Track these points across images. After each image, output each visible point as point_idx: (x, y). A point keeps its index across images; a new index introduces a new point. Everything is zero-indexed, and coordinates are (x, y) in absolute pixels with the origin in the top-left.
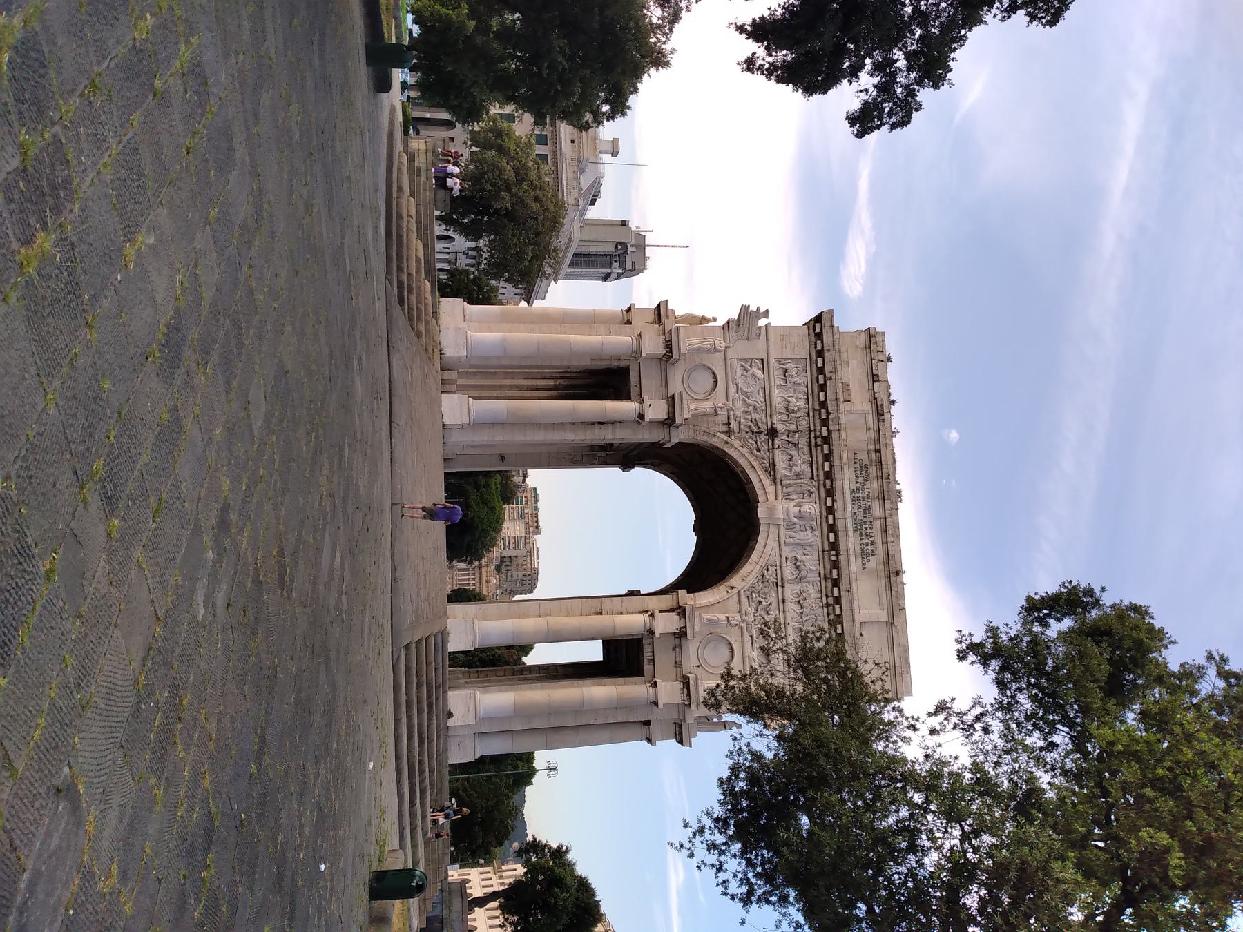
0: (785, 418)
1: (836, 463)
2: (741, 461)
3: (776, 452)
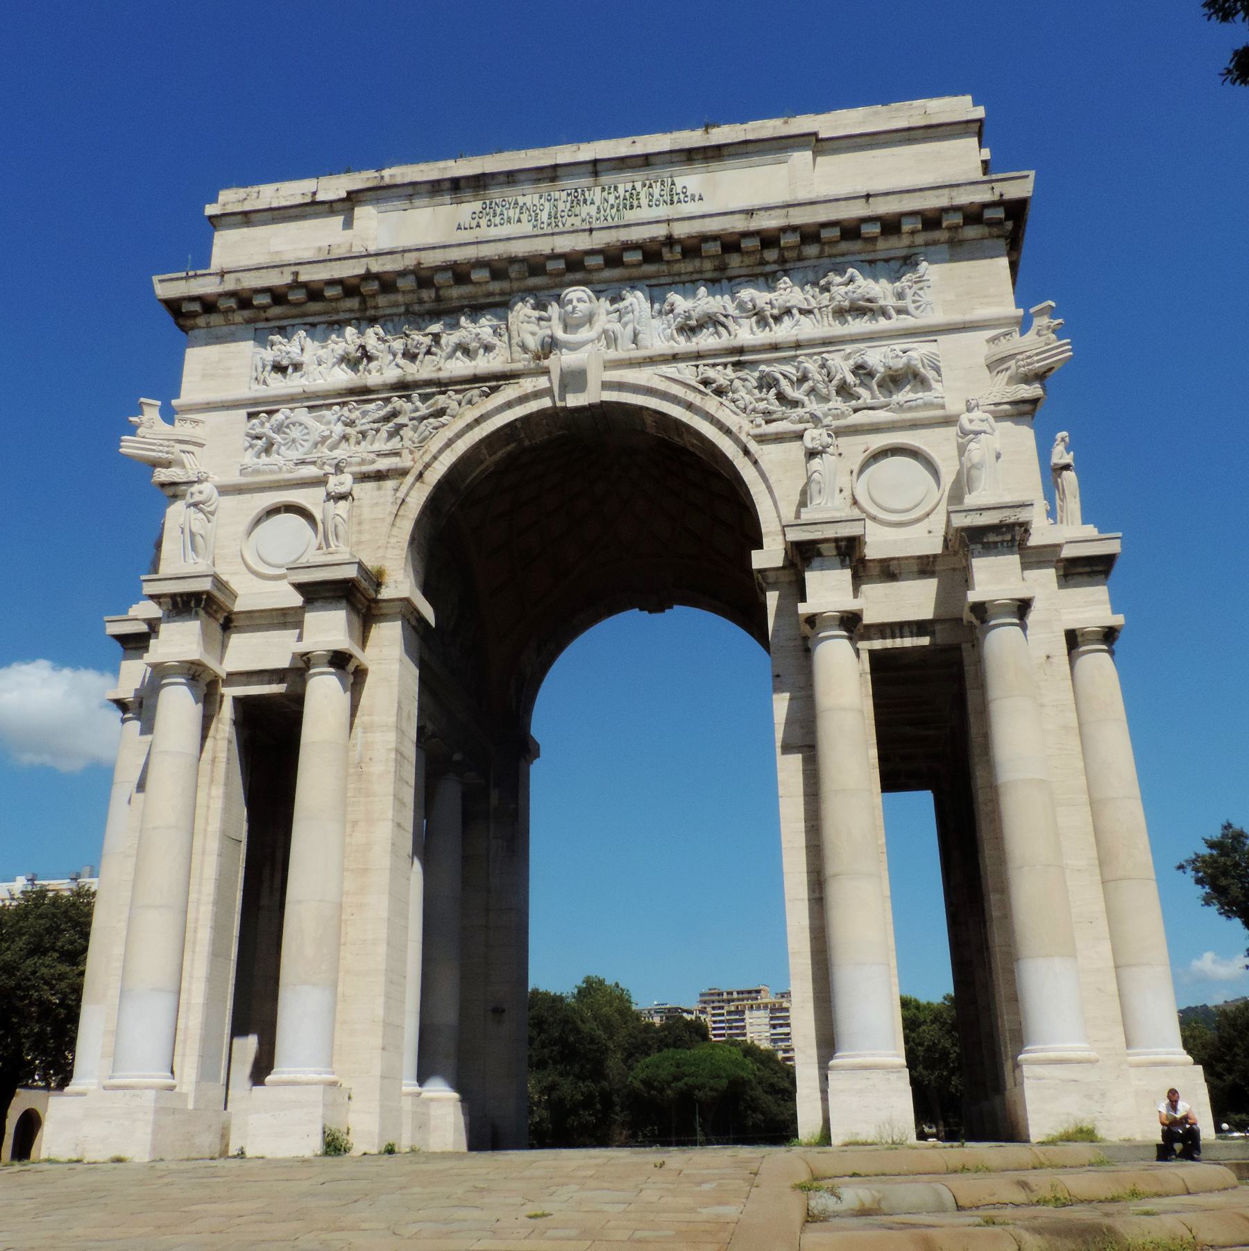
0: (373, 365)
1: (470, 253)
2: (462, 447)
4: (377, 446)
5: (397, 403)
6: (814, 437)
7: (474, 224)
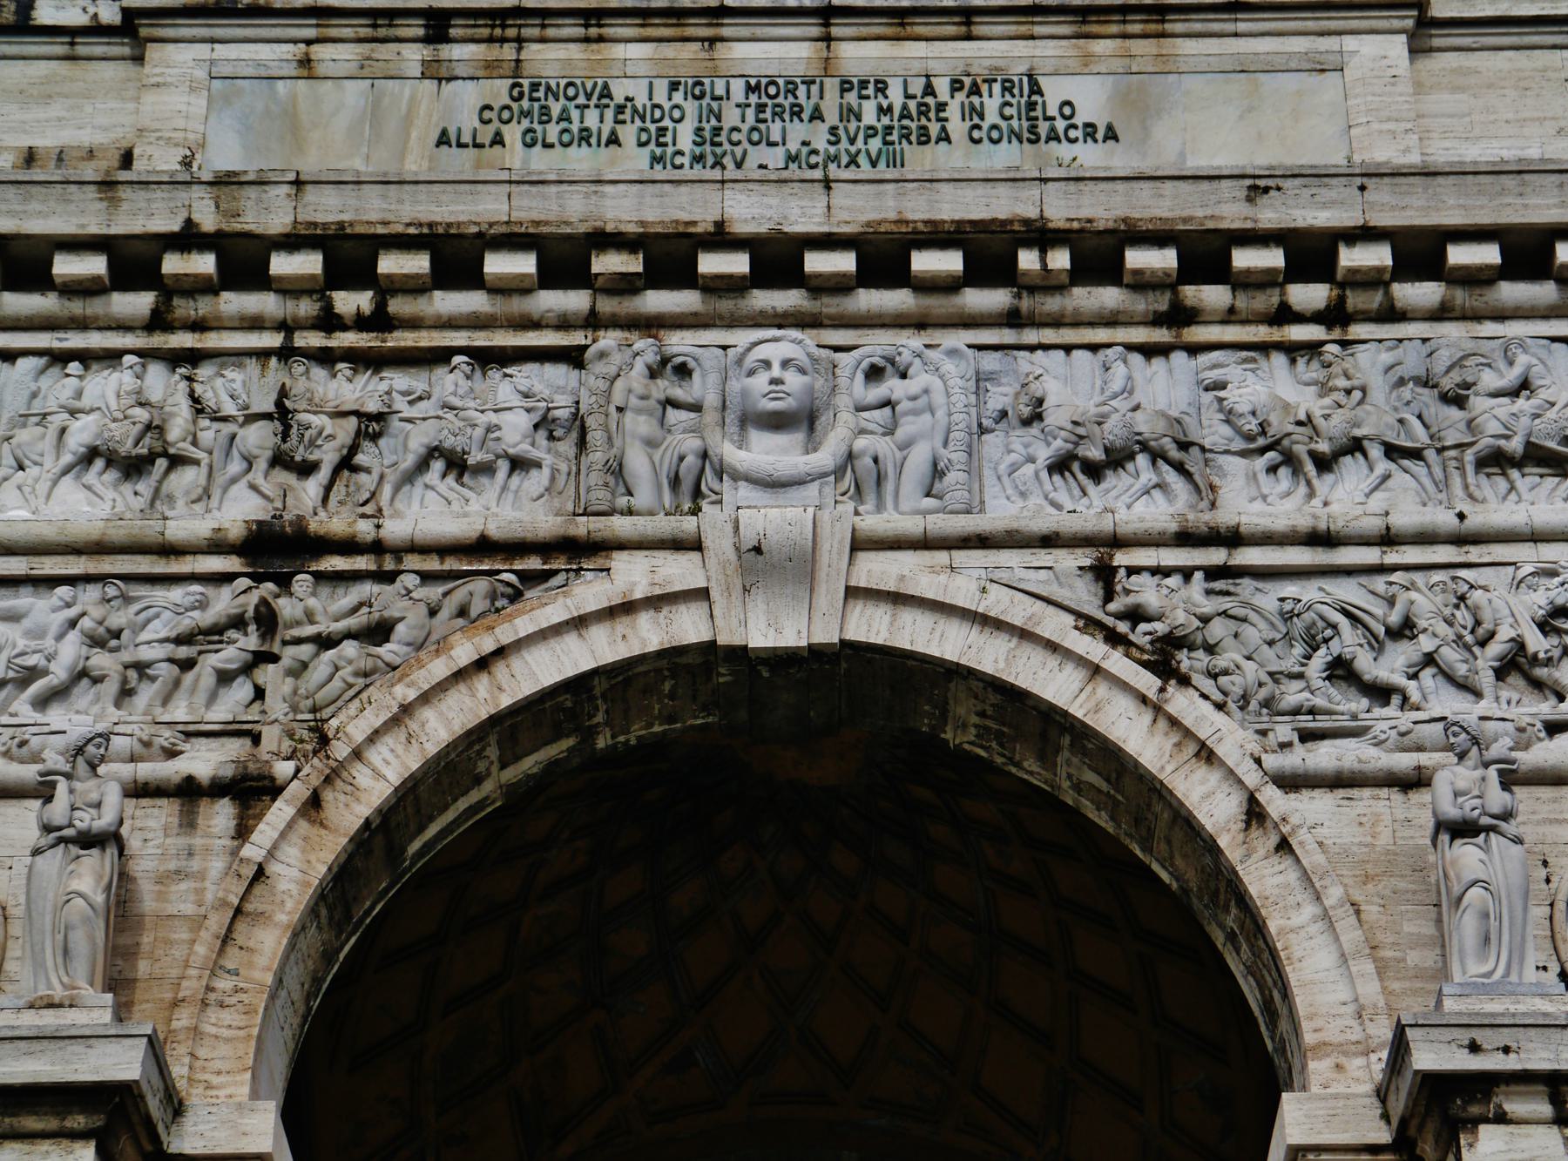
0: (186, 478)
2: (441, 726)
3: (395, 529)
4: (180, 711)
6: (1459, 785)
7: (486, 136)
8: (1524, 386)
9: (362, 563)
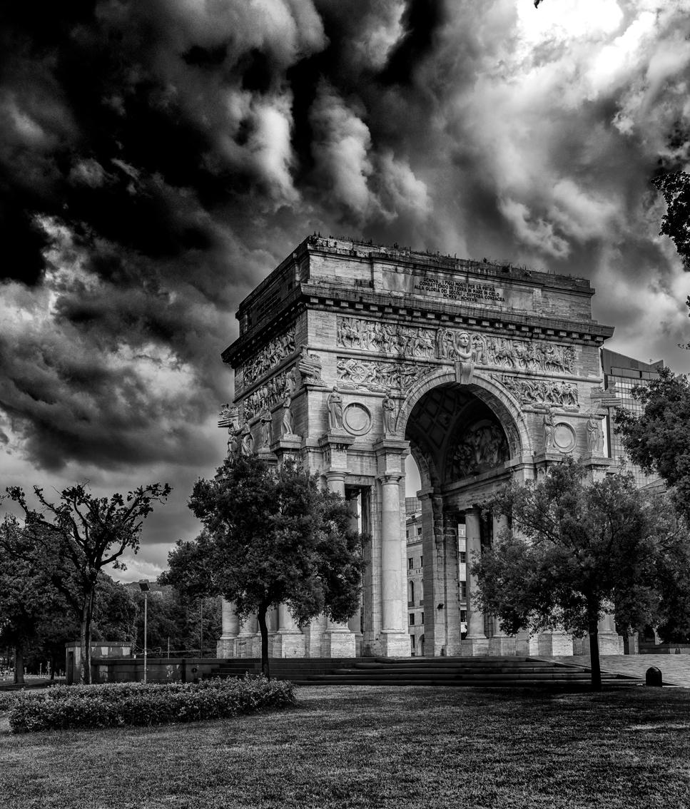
0: (386, 345)
1: (430, 307)
2: (423, 391)
3: (416, 359)
5: (398, 367)
8: (552, 353)
9: (411, 363)
